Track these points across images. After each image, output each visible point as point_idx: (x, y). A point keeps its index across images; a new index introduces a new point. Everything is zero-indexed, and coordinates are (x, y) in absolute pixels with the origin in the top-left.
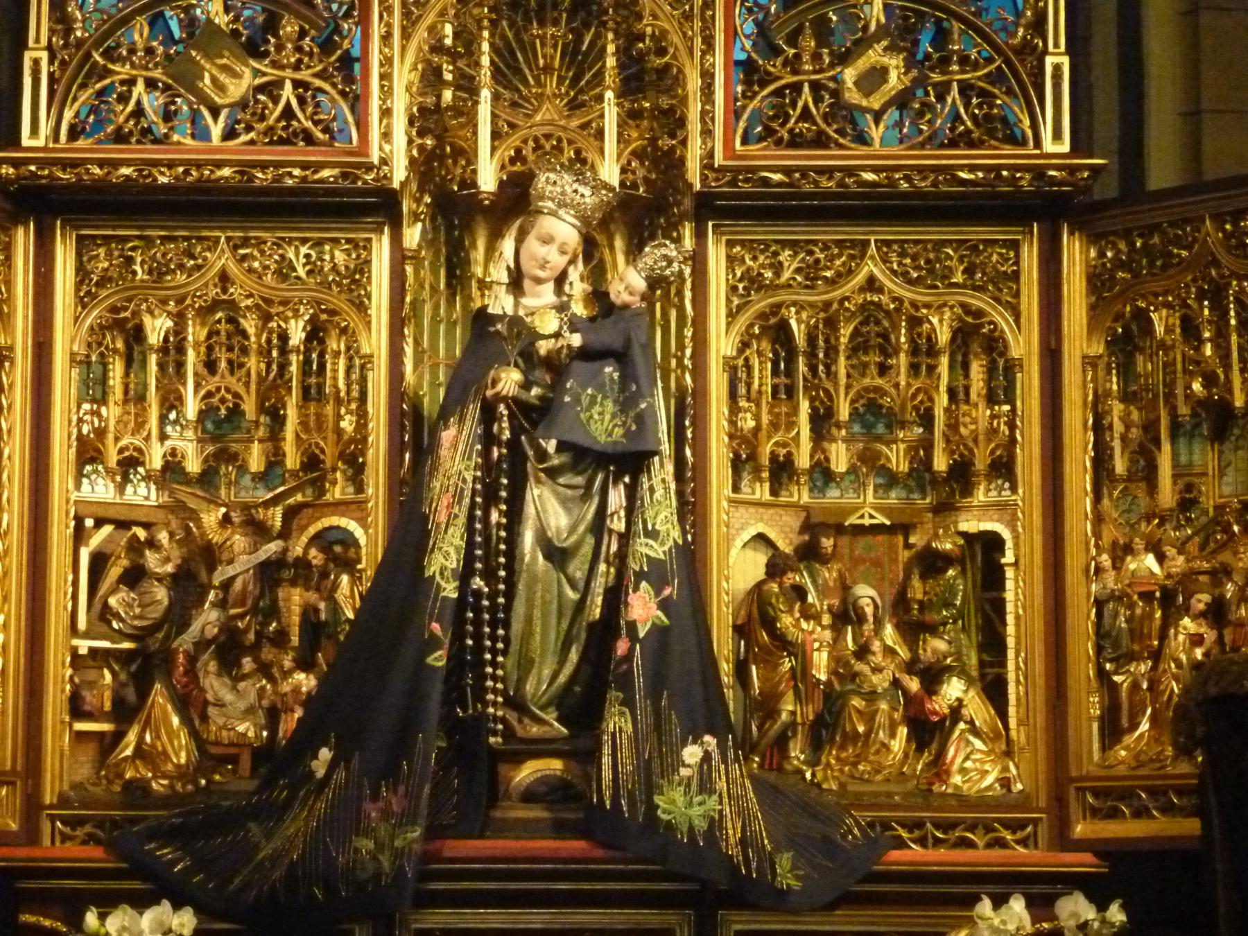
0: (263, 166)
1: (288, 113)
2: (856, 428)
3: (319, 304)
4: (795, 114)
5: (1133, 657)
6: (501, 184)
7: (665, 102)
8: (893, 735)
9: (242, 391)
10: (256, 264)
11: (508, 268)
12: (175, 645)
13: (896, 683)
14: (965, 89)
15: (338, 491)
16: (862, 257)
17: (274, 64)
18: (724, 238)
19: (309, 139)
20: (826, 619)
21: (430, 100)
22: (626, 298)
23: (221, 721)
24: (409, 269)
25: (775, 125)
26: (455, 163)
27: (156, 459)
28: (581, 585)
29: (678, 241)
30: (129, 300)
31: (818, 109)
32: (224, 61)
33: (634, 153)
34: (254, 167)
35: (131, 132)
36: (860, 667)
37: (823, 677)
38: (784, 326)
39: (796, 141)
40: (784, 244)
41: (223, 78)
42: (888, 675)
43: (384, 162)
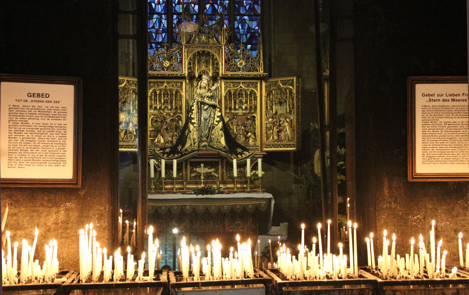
1: (174, 68)
5: (270, 130)
14: (251, 65)
15: (179, 111)
17: (172, 62)
39: (232, 71)
40: (231, 82)
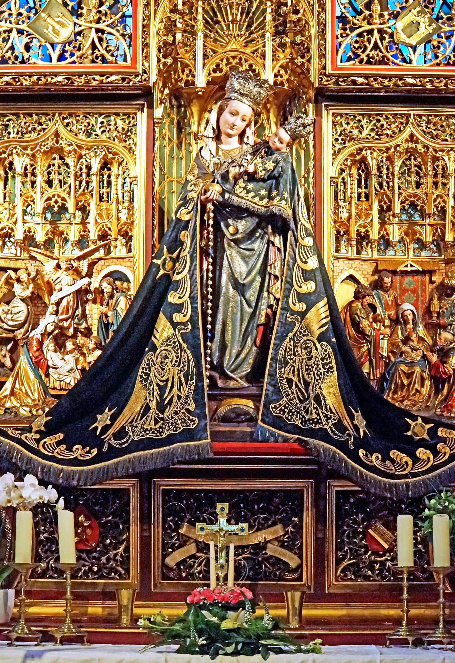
0: (80, 75)
1: (94, 46)
2: (404, 217)
3: (108, 149)
4: (370, 47)
6: (209, 83)
7: (298, 39)
8: (422, 385)
9: (66, 197)
10: (74, 128)
11: (213, 129)
12: (31, 335)
13: (424, 357)
16: (407, 124)
18: (331, 113)
19: (104, 60)
20: (387, 323)
21: (170, 38)
22: (278, 145)
23: (56, 376)
24: (157, 130)
25: (359, 52)
26: (183, 72)
27: (19, 235)
28: (253, 304)
29: (306, 113)
30: (7, 147)
31: (382, 44)
32: (59, 19)
33: (281, 66)
34: (75, 76)
35: (9, 58)
36: (405, 348)
37: (385, 354)
38: (363, 160)
40: (363, 115)
41: (57, 27)
42: (420, 353)
43: (145, 72)
